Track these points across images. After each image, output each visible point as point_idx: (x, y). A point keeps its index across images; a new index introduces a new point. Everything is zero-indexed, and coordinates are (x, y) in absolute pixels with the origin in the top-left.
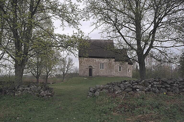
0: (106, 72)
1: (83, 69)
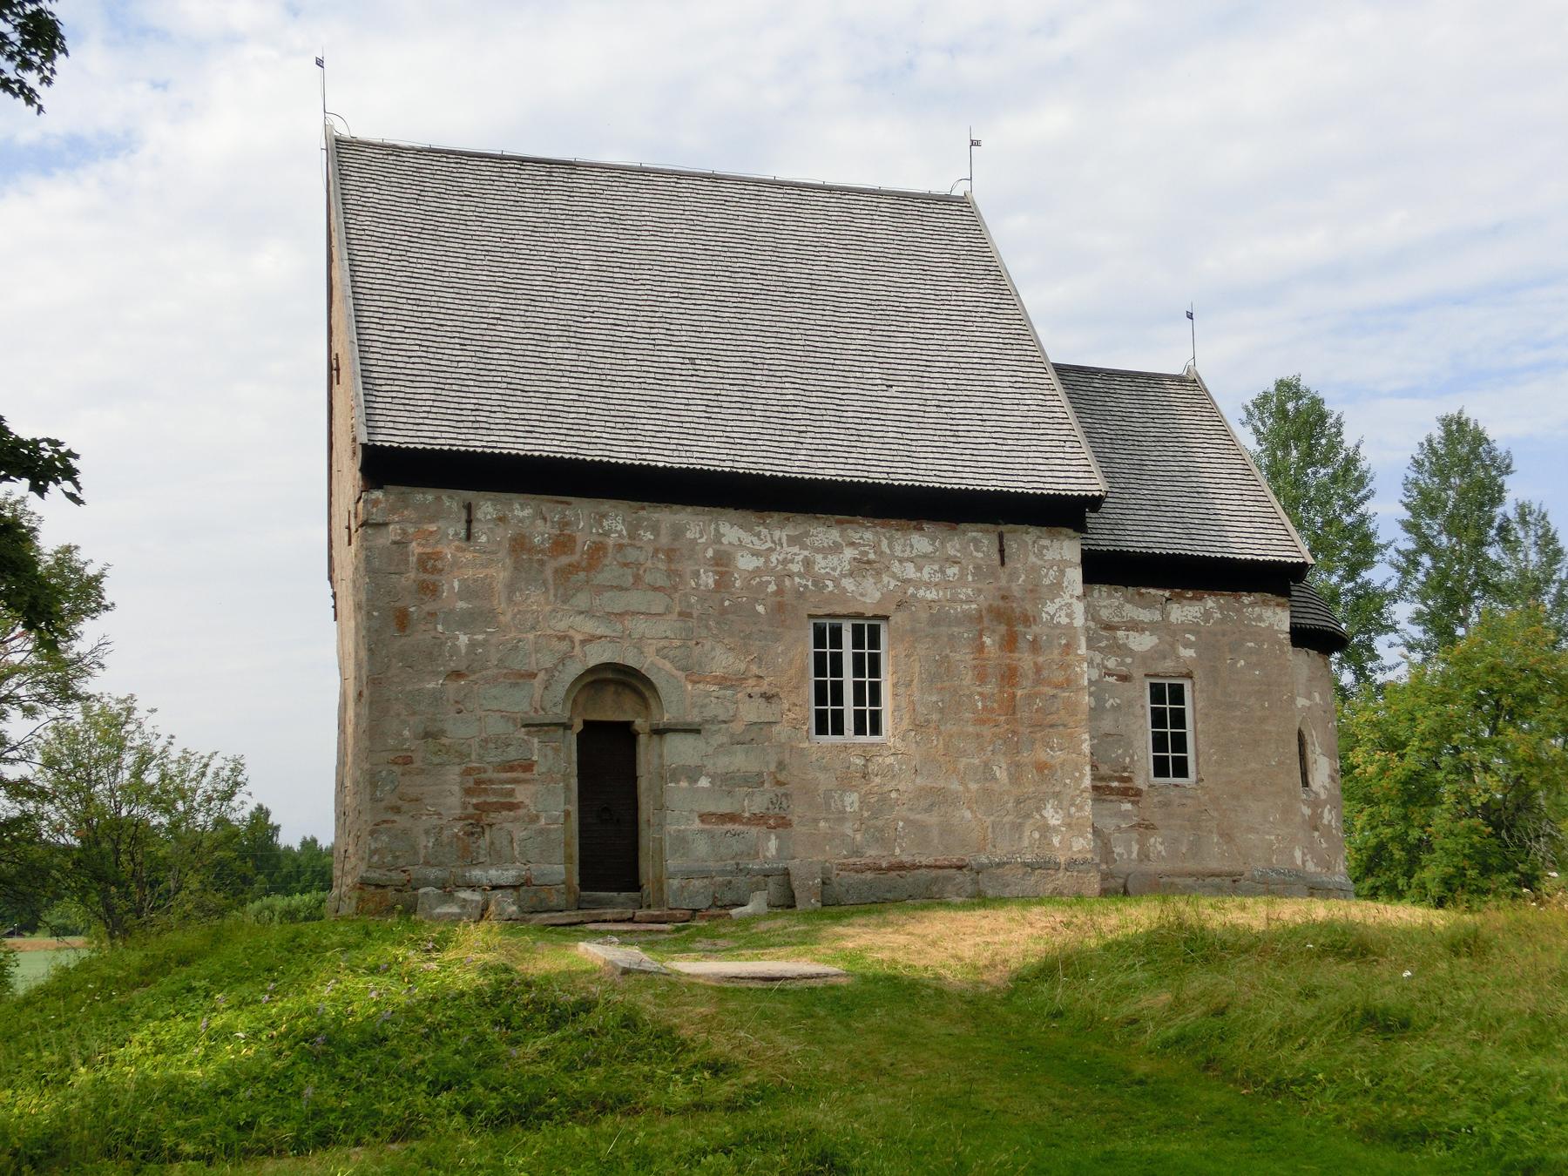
1: (458, 731)
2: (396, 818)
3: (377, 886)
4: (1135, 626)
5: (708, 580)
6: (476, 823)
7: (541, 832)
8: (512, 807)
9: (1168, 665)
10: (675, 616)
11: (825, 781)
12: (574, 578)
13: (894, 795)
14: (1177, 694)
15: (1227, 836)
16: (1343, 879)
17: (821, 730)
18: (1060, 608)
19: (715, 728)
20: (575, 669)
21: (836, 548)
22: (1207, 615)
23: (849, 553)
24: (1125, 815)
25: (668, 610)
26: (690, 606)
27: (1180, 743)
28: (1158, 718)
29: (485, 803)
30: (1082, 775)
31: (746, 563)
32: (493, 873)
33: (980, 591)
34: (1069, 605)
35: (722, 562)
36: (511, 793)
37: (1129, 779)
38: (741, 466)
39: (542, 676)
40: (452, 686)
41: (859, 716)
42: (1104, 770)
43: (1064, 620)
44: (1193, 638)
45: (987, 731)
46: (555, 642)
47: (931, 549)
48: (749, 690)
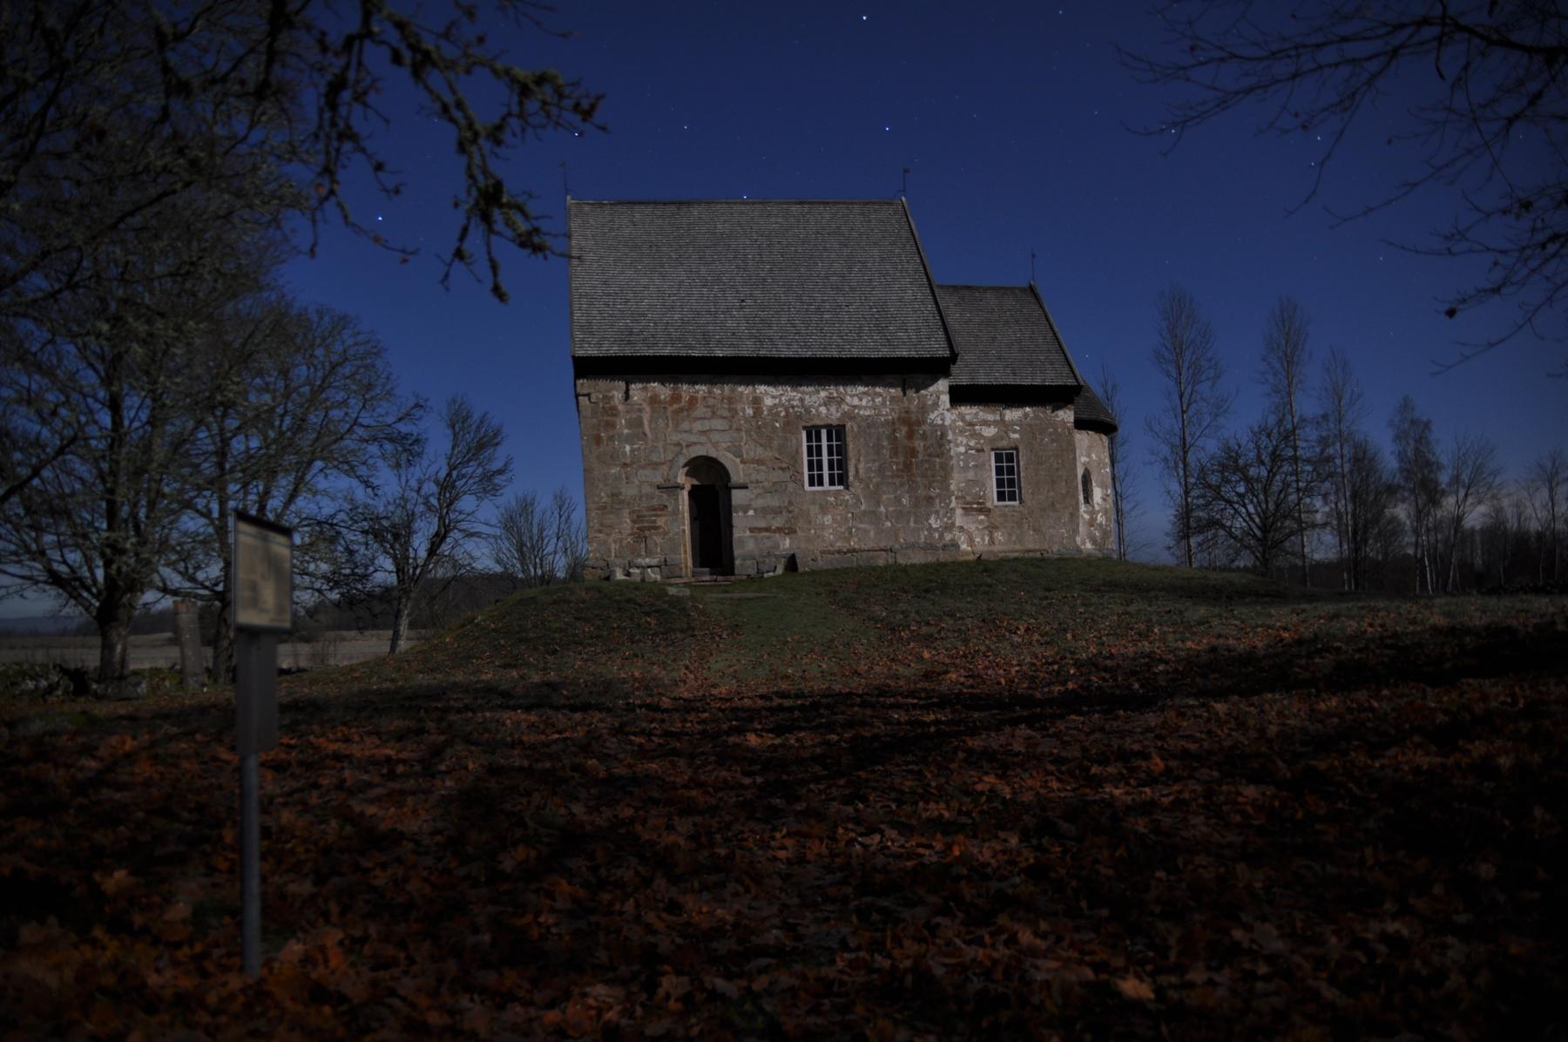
0: (873, 516)
1: (629, 491)
4: (986, 423)
5: (750, 412)
8: (656, 528)
9: (1004, 443)
14: (1010, 458)
17: (812, 484)
20: (682, 461)
22: (1026, 415)
24: (981, 522)
28: (999, 471)
31: (769, 402)
35: (757, 401)
38: (762, 353)
45: (897, 481)
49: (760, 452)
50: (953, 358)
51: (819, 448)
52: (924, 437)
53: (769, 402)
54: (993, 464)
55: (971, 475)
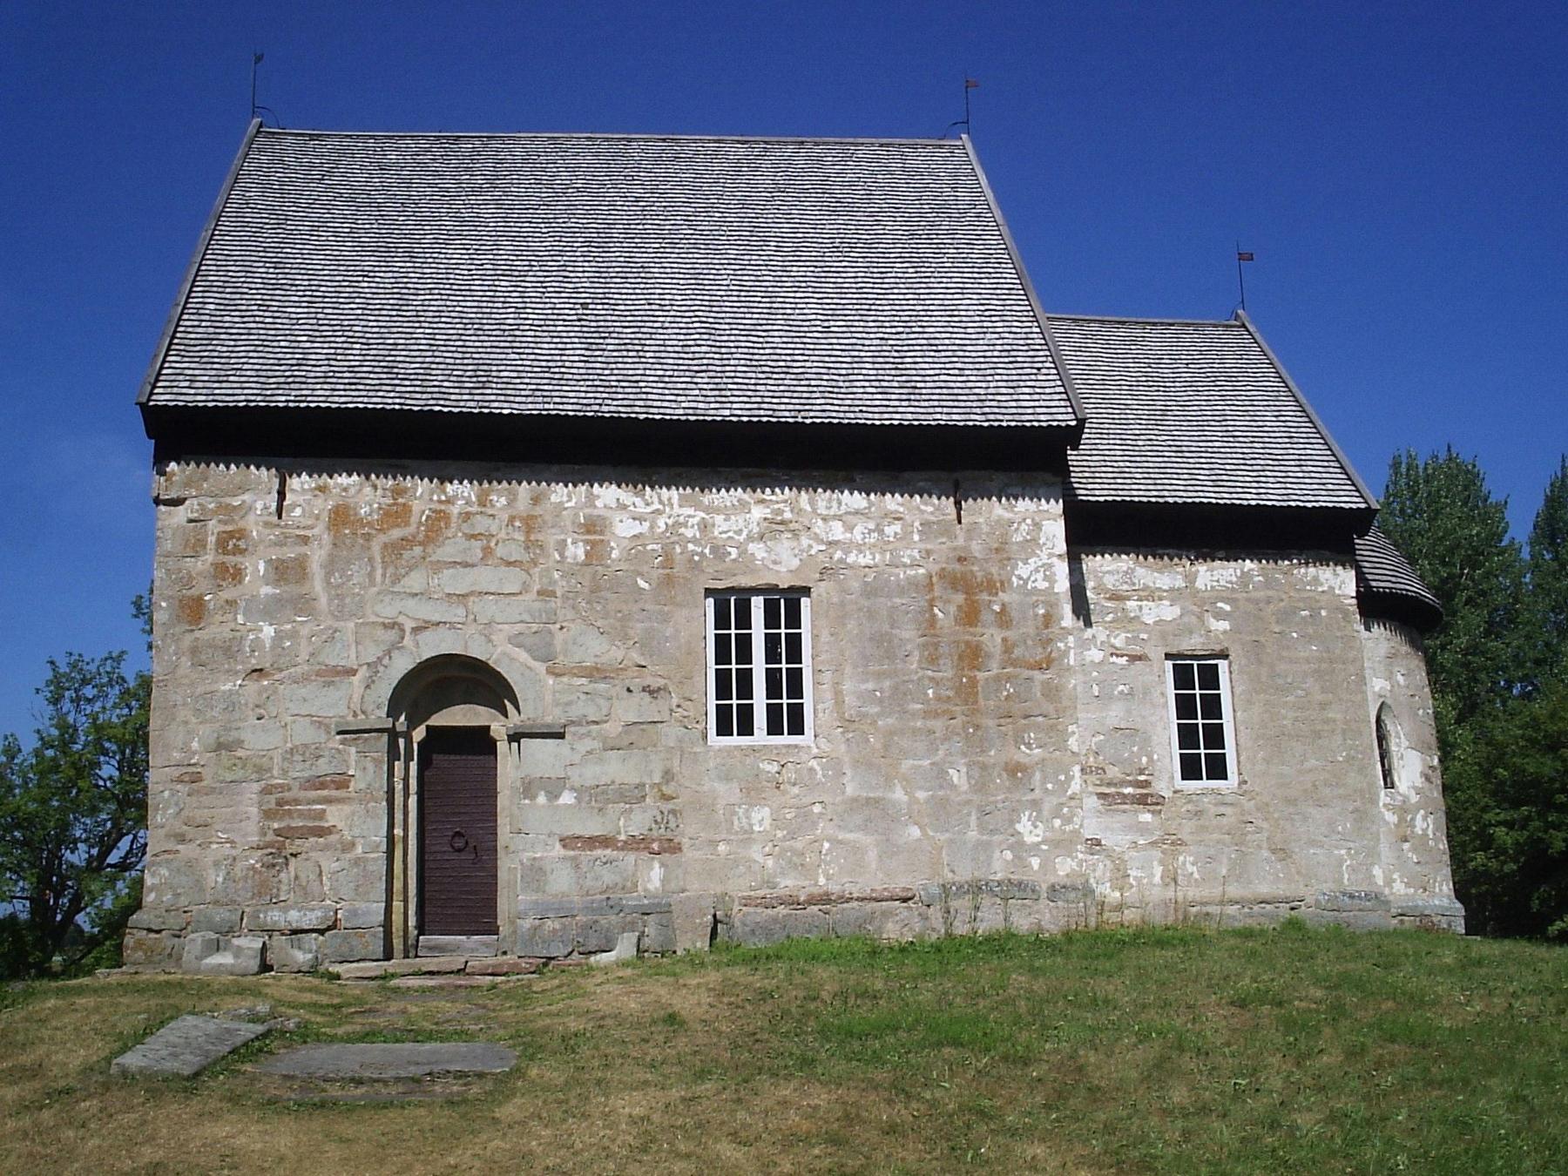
0: (872, 811)
1: (257, 739)
2: (180, 847)
3: (150, 930)
4: (1151, 594)
5: (577, 552)
6: (278, 852)
7: (357, 862)
8: (321, 832)
9: (1193, 643)
10: (533, 595)
11: (727, 793)
12: (407, 554)
13: (817, 809)
14: (1210, 677)
15: (1282, 852)
16: (1446, 902)
17: (724, 729)
18: (1037, 570)
19: (583, 730)
20: (402, 665)
21: (744, 507)
22: (1245, 577)
23: (758, 513)
24: (1143, 829)
25: (525, 588)
26: (553, 582)
27: (1215, 736)
28: (1185, 707)
29: (290, 828)
30: (1070, 779)
31: (625, 528)
32: (293, 915)
33: (928, 553)
34: (1051, 566)
35: (593, 528)
36: (321, 815)
37: (1147, 784)
38: (607, 410)
39: (363, 672)
40: (252, 686)
41: (773, 713)
42: (1114, 772)
43: (1043, 585)
44: (1228, 608)
45: (938, 724)
46: (380, 632)
47: (864, 504)
48: (627, 683)
49: (595, 648)
50: (1072, 435)
51: (745, 643)
52: (1003, 619)
53: (625, 528)
54: (1171, 692)
55: (1115, 715)
